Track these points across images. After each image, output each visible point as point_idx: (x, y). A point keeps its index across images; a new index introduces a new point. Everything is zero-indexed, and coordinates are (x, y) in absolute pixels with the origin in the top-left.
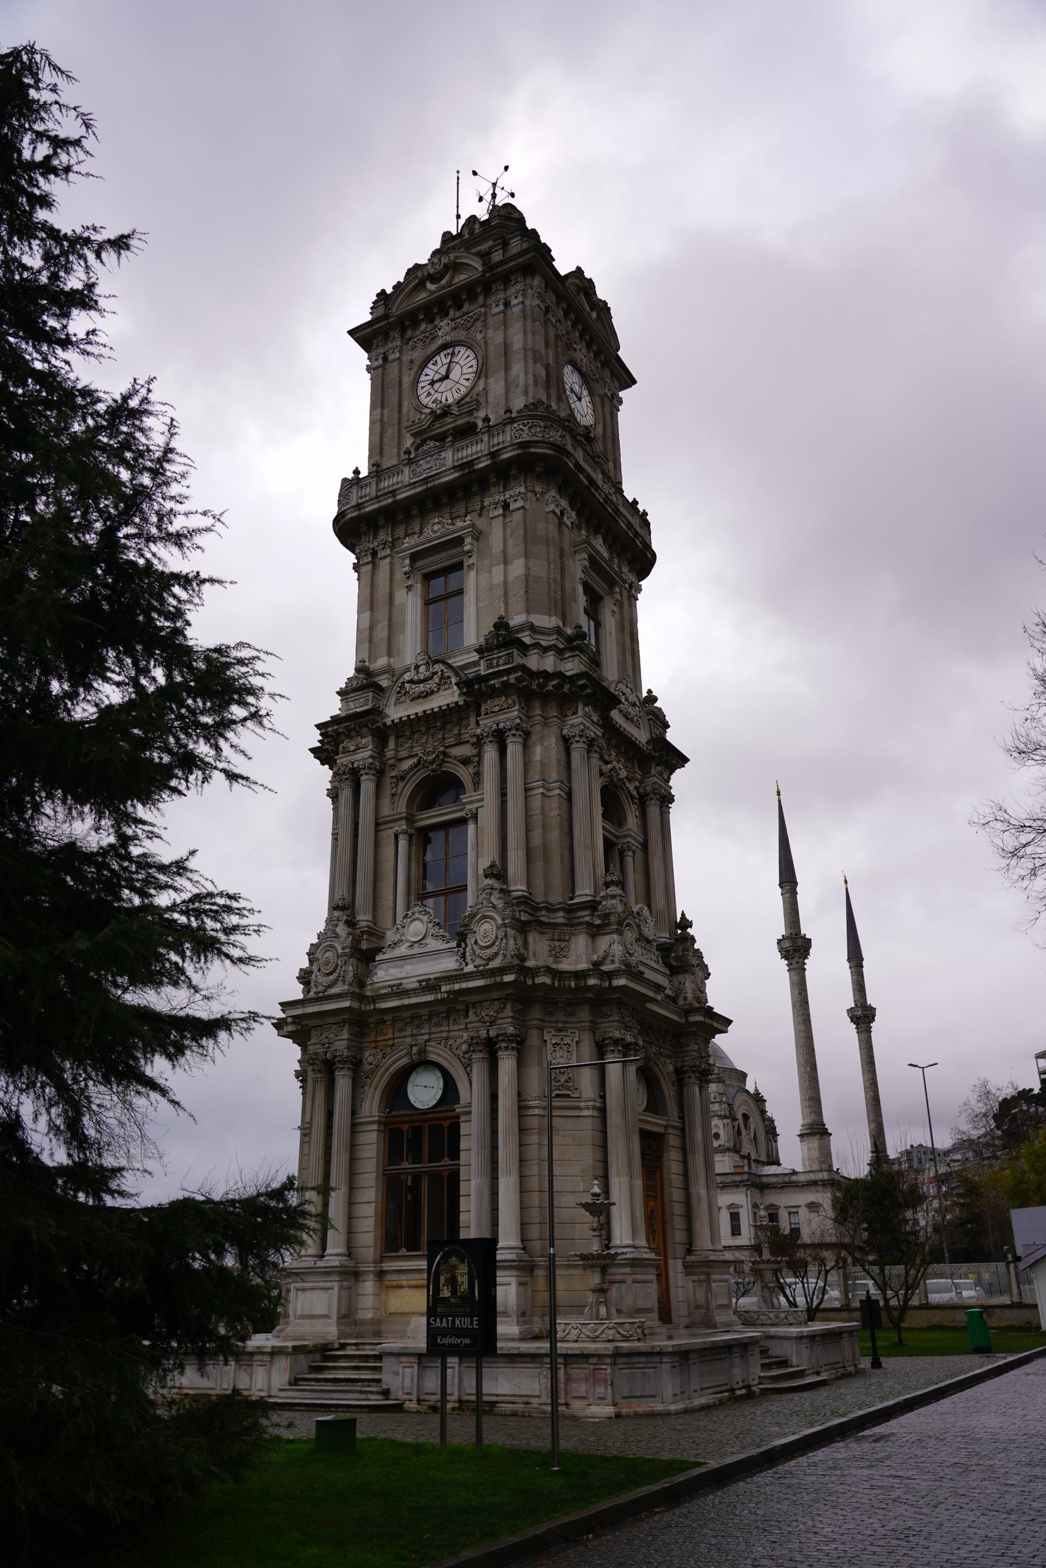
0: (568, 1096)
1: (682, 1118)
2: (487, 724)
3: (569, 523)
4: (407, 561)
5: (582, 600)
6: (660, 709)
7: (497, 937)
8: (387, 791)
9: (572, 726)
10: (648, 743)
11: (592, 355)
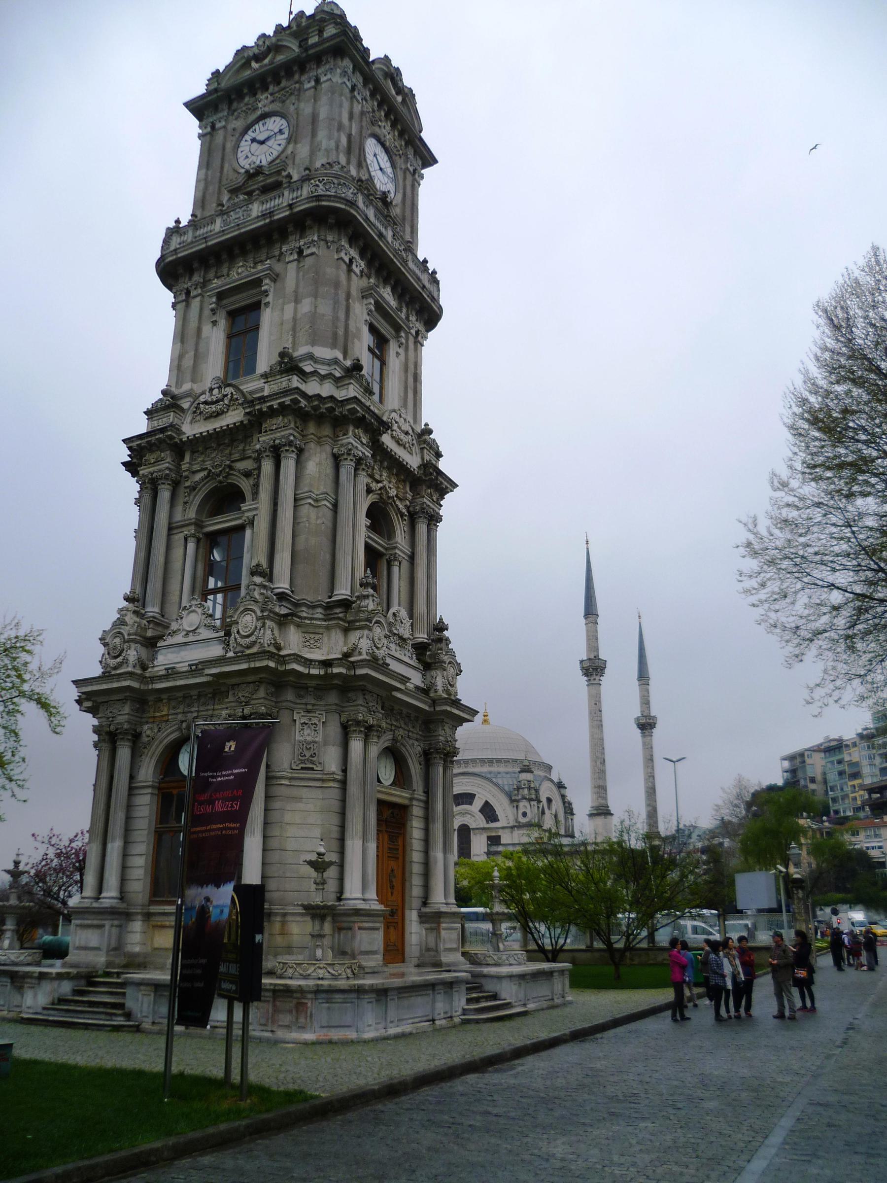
0: (312, 769)
1: (426, 793)
3: (357, 271)
4: (214, 299)
5: (367, 339)
6: (434, 440)
7: (256, 628)
8: (181, 500)
9: (342, 445)
10: (419, 467)
11: (396, 133)
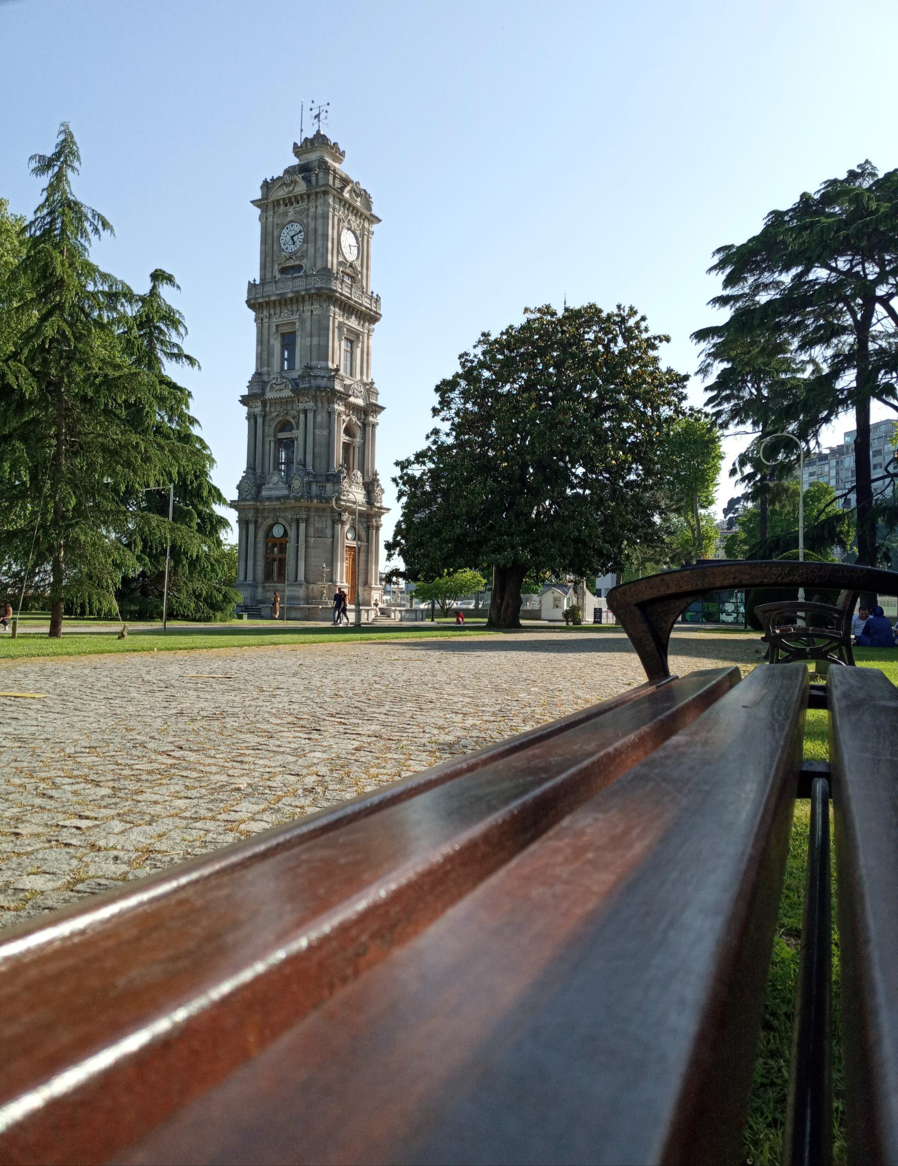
2: (301, 406)
